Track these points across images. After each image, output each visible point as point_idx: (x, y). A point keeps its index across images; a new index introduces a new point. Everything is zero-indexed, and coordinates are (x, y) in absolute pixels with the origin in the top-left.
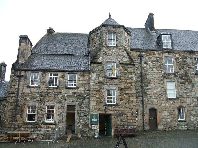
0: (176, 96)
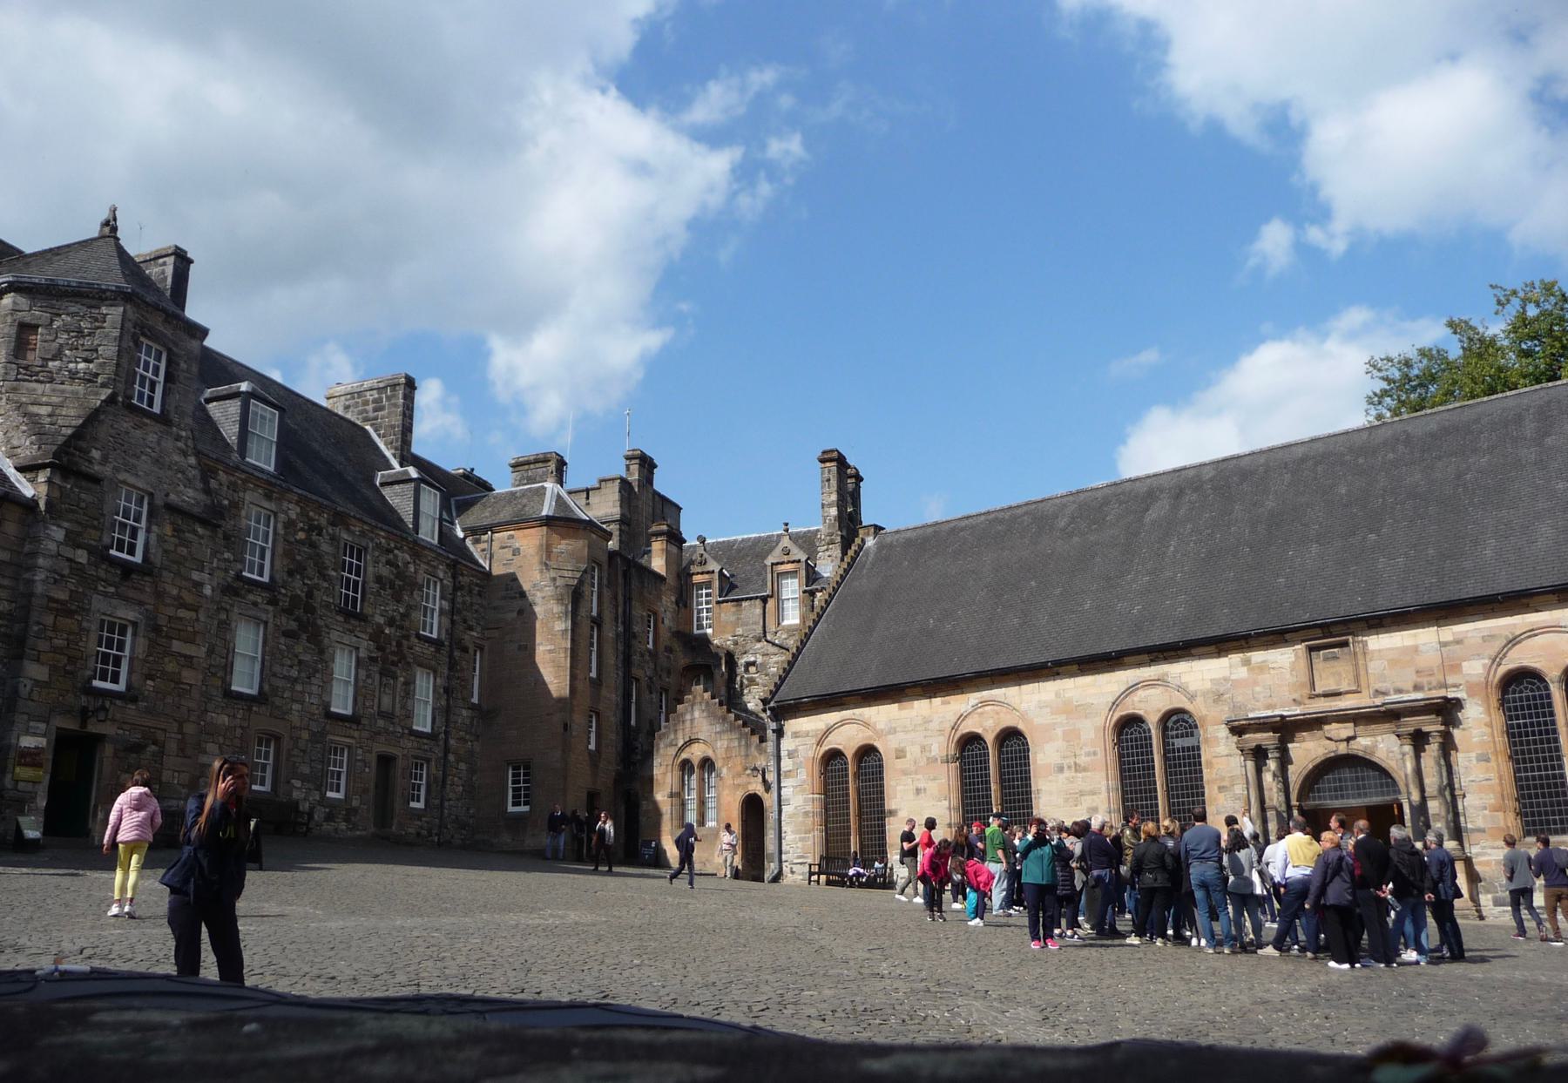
0: (256, 686)
